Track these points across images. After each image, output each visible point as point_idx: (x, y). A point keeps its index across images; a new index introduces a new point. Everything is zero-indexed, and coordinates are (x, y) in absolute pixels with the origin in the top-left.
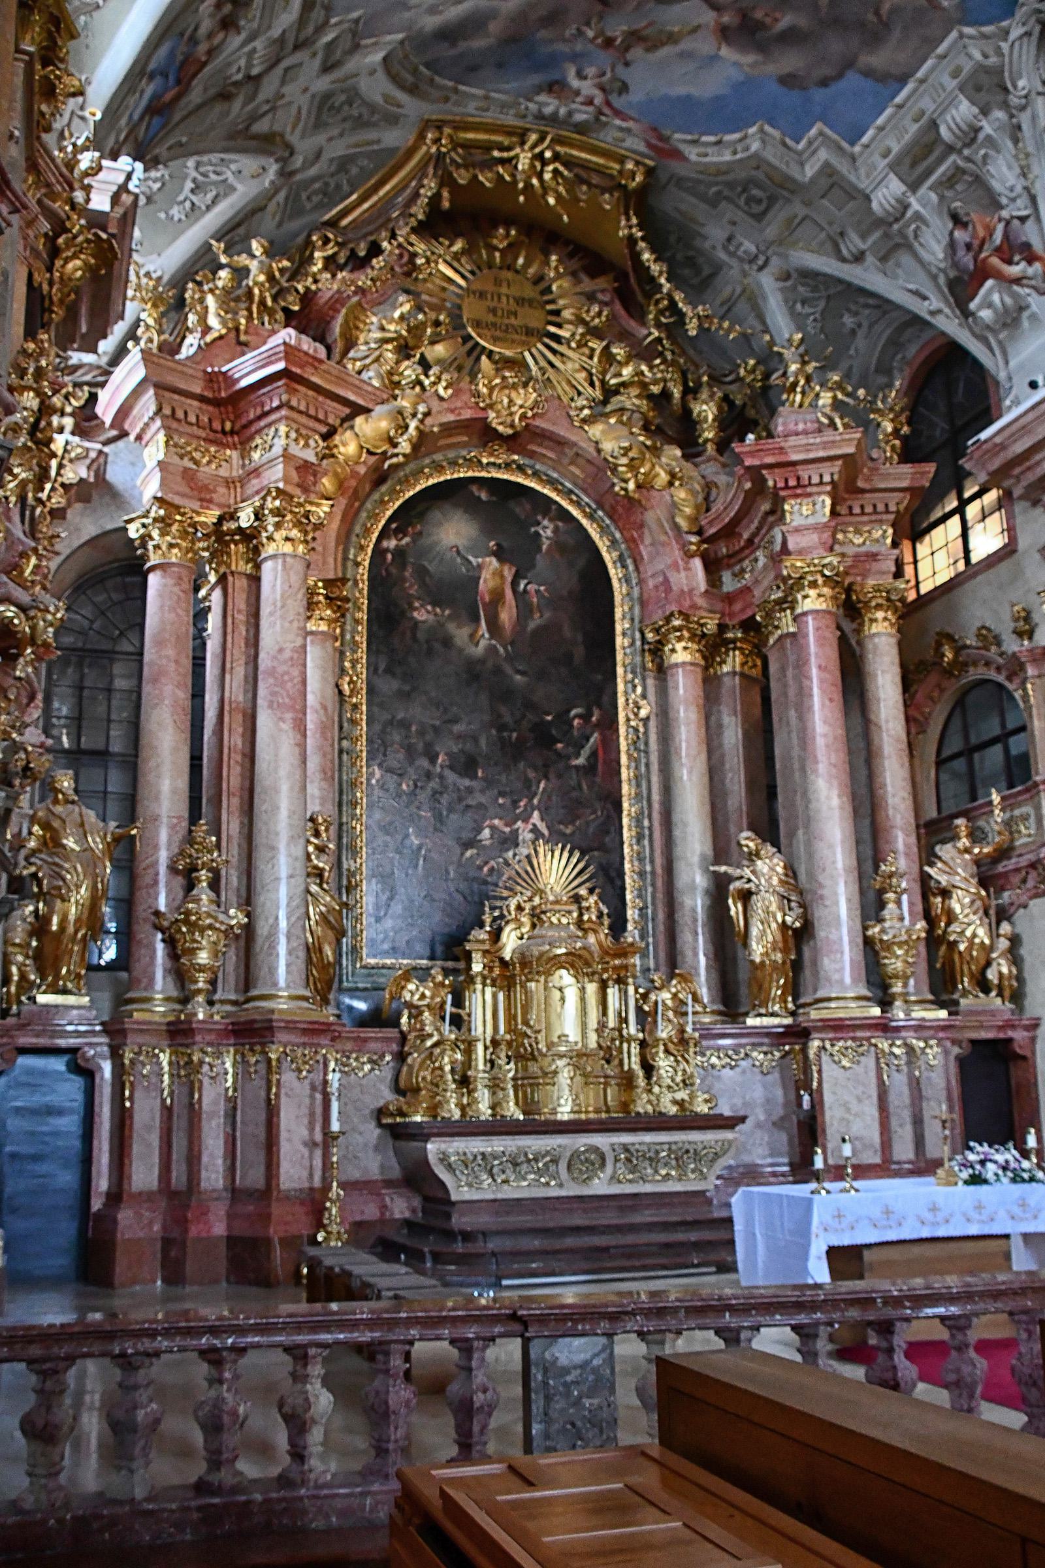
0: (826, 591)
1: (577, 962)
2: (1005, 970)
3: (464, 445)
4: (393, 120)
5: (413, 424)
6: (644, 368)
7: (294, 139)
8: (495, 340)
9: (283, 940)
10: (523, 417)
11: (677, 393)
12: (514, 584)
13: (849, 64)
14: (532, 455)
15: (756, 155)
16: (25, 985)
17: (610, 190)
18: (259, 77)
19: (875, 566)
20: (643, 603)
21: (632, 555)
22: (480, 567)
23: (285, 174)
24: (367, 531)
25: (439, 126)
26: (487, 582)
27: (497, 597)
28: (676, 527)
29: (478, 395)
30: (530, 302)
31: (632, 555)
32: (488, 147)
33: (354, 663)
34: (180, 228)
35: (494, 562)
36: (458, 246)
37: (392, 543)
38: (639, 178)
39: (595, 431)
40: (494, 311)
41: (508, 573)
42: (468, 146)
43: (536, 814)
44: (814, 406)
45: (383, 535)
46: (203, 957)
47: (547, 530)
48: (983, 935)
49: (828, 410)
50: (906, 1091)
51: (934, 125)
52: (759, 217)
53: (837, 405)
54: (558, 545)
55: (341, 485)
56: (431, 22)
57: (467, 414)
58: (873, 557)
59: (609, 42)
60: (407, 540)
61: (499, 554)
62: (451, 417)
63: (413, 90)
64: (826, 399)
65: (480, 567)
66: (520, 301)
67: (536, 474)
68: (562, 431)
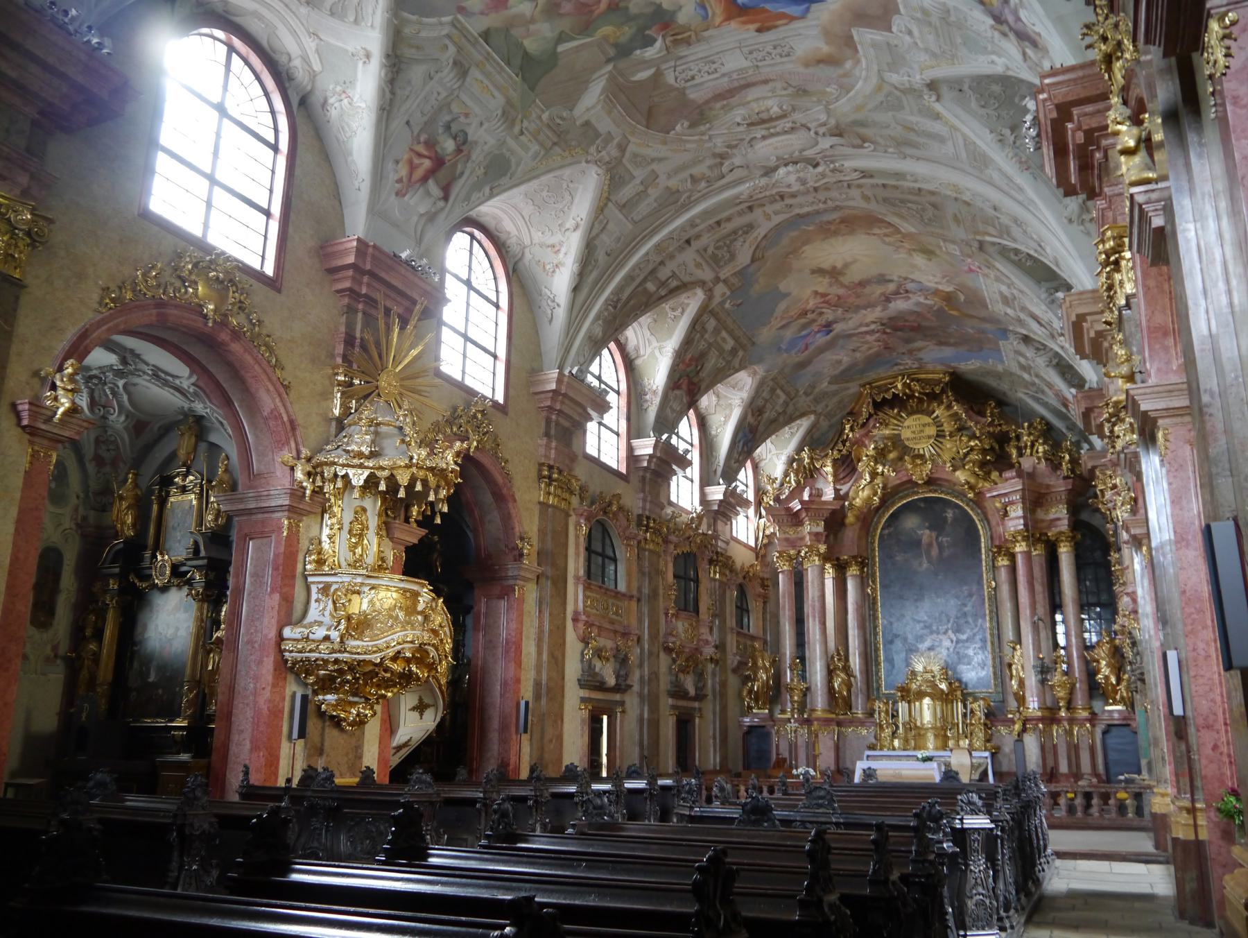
0: (1024, 544)
1: (938, 696)
2: (1125, 694)
3: (907, 489)
4: (849, 388)
5: (879, 491)
6: (977, 442)
7: (813, 408)
8: (916, 444)
9: (819, 693)
10: (927, 475)
11: (997, 447)
12: (937, 538)
13: (981, 349)
14: (940, 485)
15: (980, 367)
16: (750, 708)
17: (939, 385)
18: (784, 412)
19: (1059, 523)
20: (992, 538)
21: (985, 518)
22: (922, 535)
23: (818, 415)
24: (875, 530)
25: (863, 386)
26: (925, 540)
27: (930, 545)
28: (996, 508)
29: (907, 470)
30: (929, 425)
31: (985, 518)
32: (885, 385)
33: (873, 582)
34: (789, 441)
35: (927, 532)
36: (896, 411)
37: (886, 532)
38: (947, 379)
39: (958, 473)
40: (914, 432)
41: (934, 534)
42: (878, 387)
43: (950, 632)
44: (1037, 452)
45: (883, 529)
46: (796, 698)
47: (950, 514)
48: (1113, 680)
49: (1040, 455)
50: (1064, 745)
51: (1019, 363)
52: (1000, 379)
53: (1045, 452)
54: (955, 519)
55: (857, 518)
56: (837, 372)
57: (905, 479)
58: (1058, 519)
59: (903, 353)
60: (892, 529)
61: (931, 528)
62: (898, 482)
63: (847, 382)
64: (1041, 449)
65: (922, 535)
66: (924, 425)
67: (942, 492)
68: (944, 476)
